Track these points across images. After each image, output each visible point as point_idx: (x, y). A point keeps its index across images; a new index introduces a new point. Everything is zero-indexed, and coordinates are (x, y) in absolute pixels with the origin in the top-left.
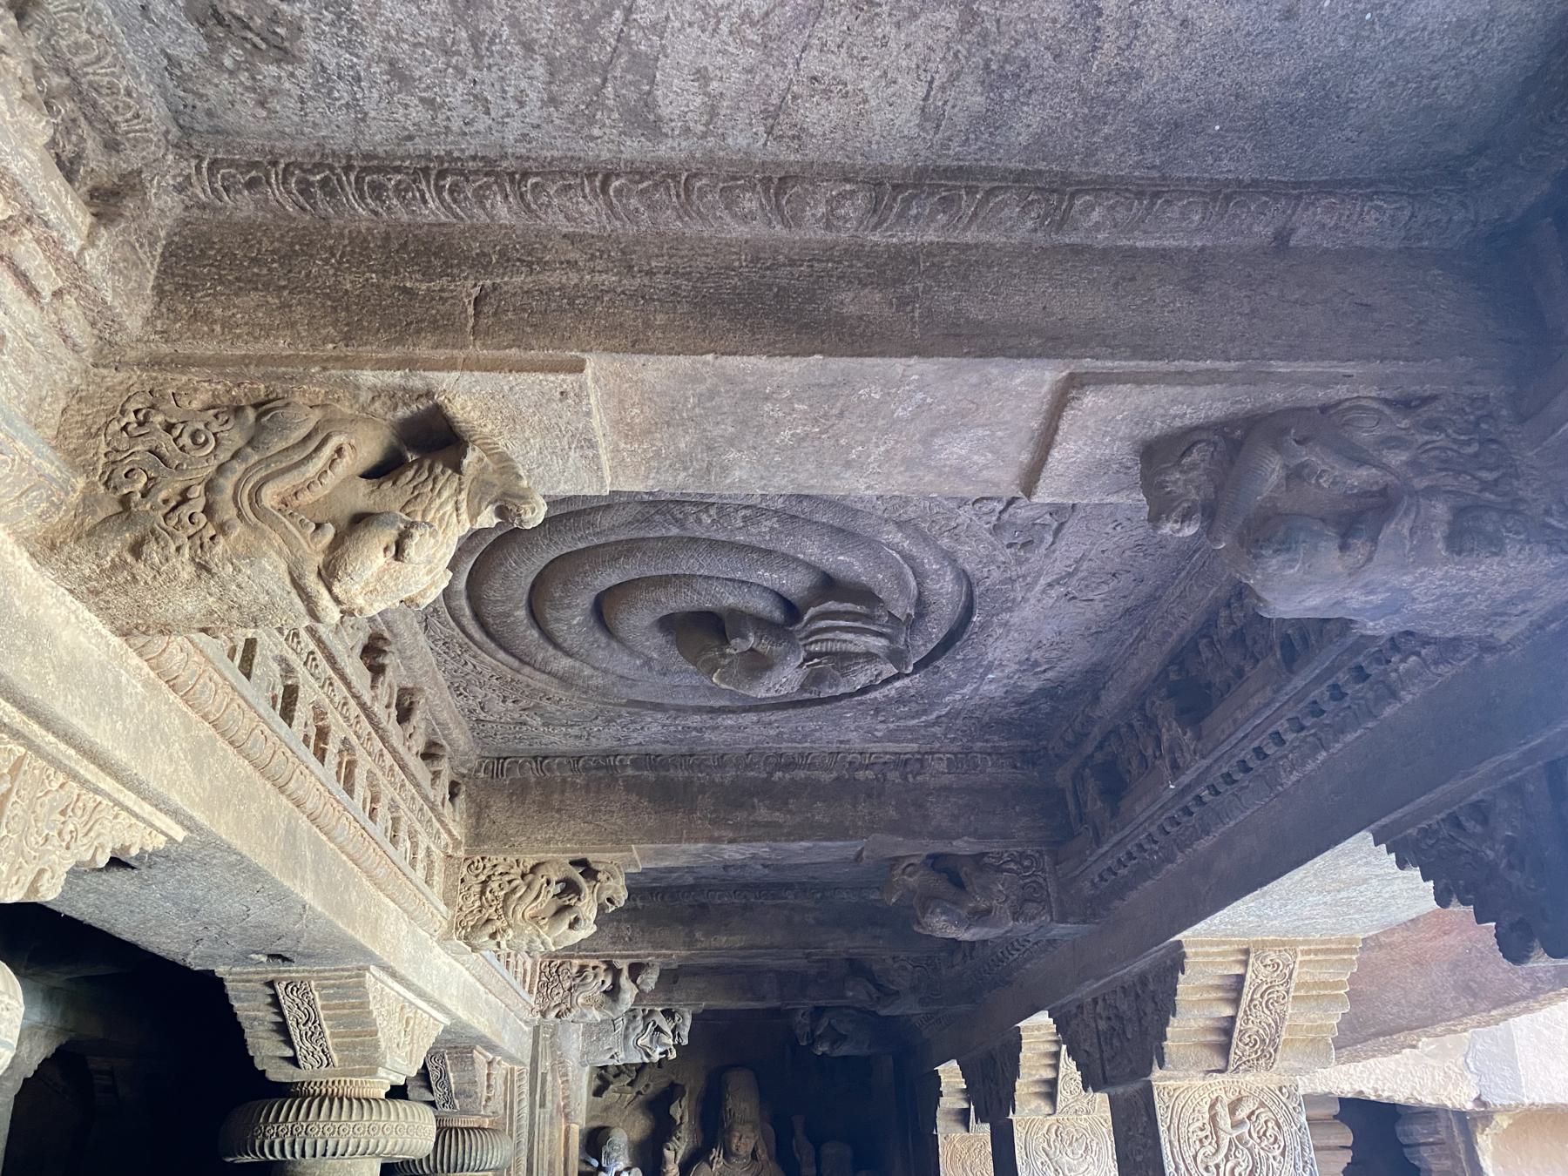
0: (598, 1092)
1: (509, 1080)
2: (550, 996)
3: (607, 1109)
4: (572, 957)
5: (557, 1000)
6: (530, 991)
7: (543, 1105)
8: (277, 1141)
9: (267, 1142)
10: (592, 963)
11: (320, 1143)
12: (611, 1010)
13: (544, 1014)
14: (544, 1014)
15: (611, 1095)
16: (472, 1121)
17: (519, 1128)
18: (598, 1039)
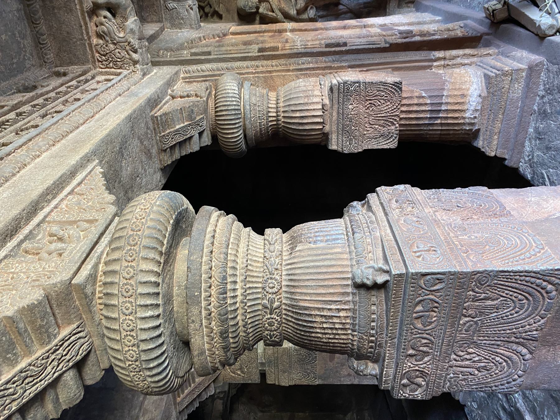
0: (220, 17)
1: (189, 80)
2: (122, 59)
3: (228, 11)
4: (90, 45)
5: (124, 53)
6: (119, 74)
7: (209, 53)
8: (150, 380)
9: (153, 385)
10: (92, 27)
11: (144, 346)
12: (126, 9)
13: (135, 62)
14: (135, 62)
15: (221, 9)
16: (211, 104)
17: (218, 70)
18: (182, 19)
